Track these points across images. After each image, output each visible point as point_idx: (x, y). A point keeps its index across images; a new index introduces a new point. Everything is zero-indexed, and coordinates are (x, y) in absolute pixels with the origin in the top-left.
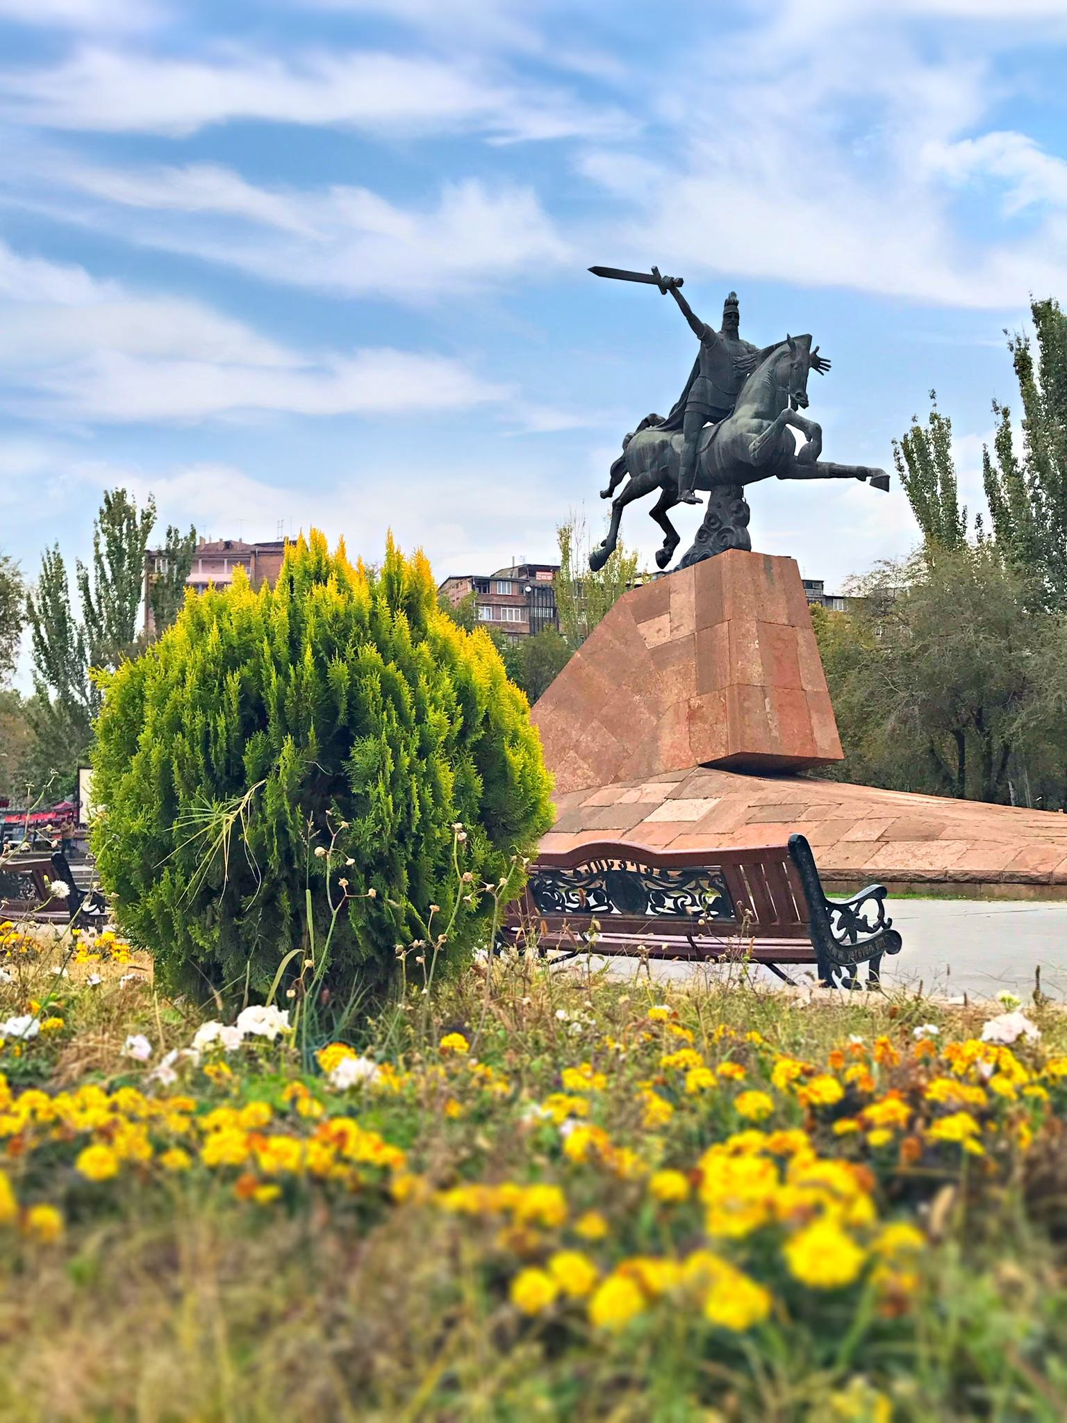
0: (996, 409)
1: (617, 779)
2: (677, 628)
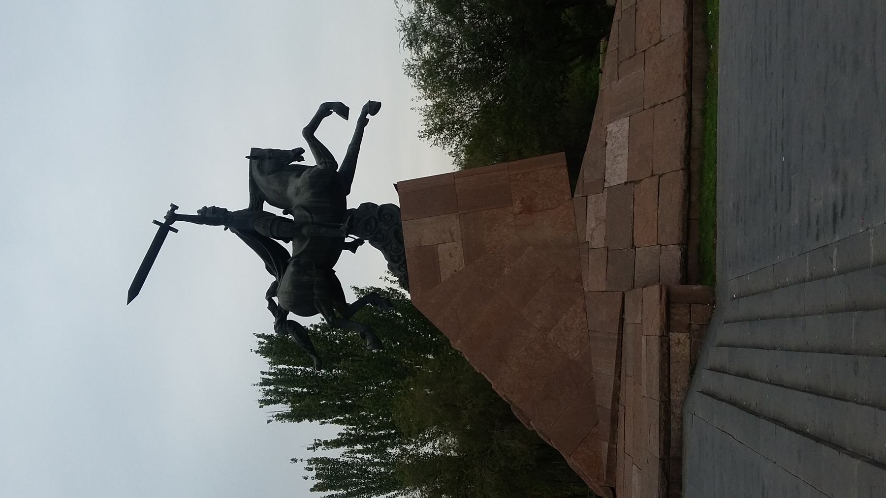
0: (313, 448)
1: (579, 280)
2: (451, 234)
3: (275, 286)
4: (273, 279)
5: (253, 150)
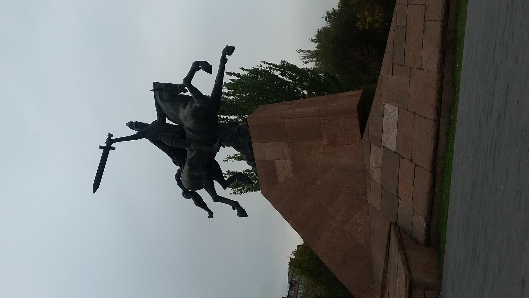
0: (227, 161)
1: (365, 194)
2: (284, 155)
3: (179, 172)
4: (179, 168)
5: (155, 84)
